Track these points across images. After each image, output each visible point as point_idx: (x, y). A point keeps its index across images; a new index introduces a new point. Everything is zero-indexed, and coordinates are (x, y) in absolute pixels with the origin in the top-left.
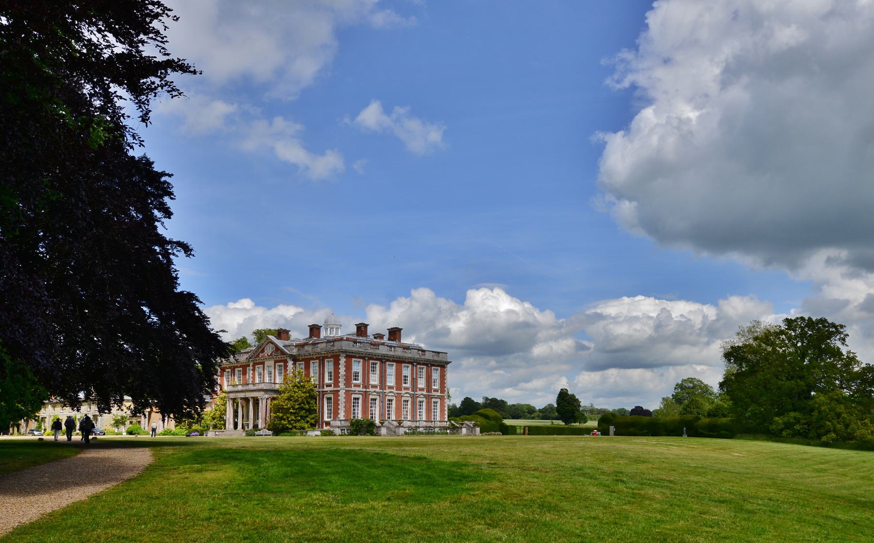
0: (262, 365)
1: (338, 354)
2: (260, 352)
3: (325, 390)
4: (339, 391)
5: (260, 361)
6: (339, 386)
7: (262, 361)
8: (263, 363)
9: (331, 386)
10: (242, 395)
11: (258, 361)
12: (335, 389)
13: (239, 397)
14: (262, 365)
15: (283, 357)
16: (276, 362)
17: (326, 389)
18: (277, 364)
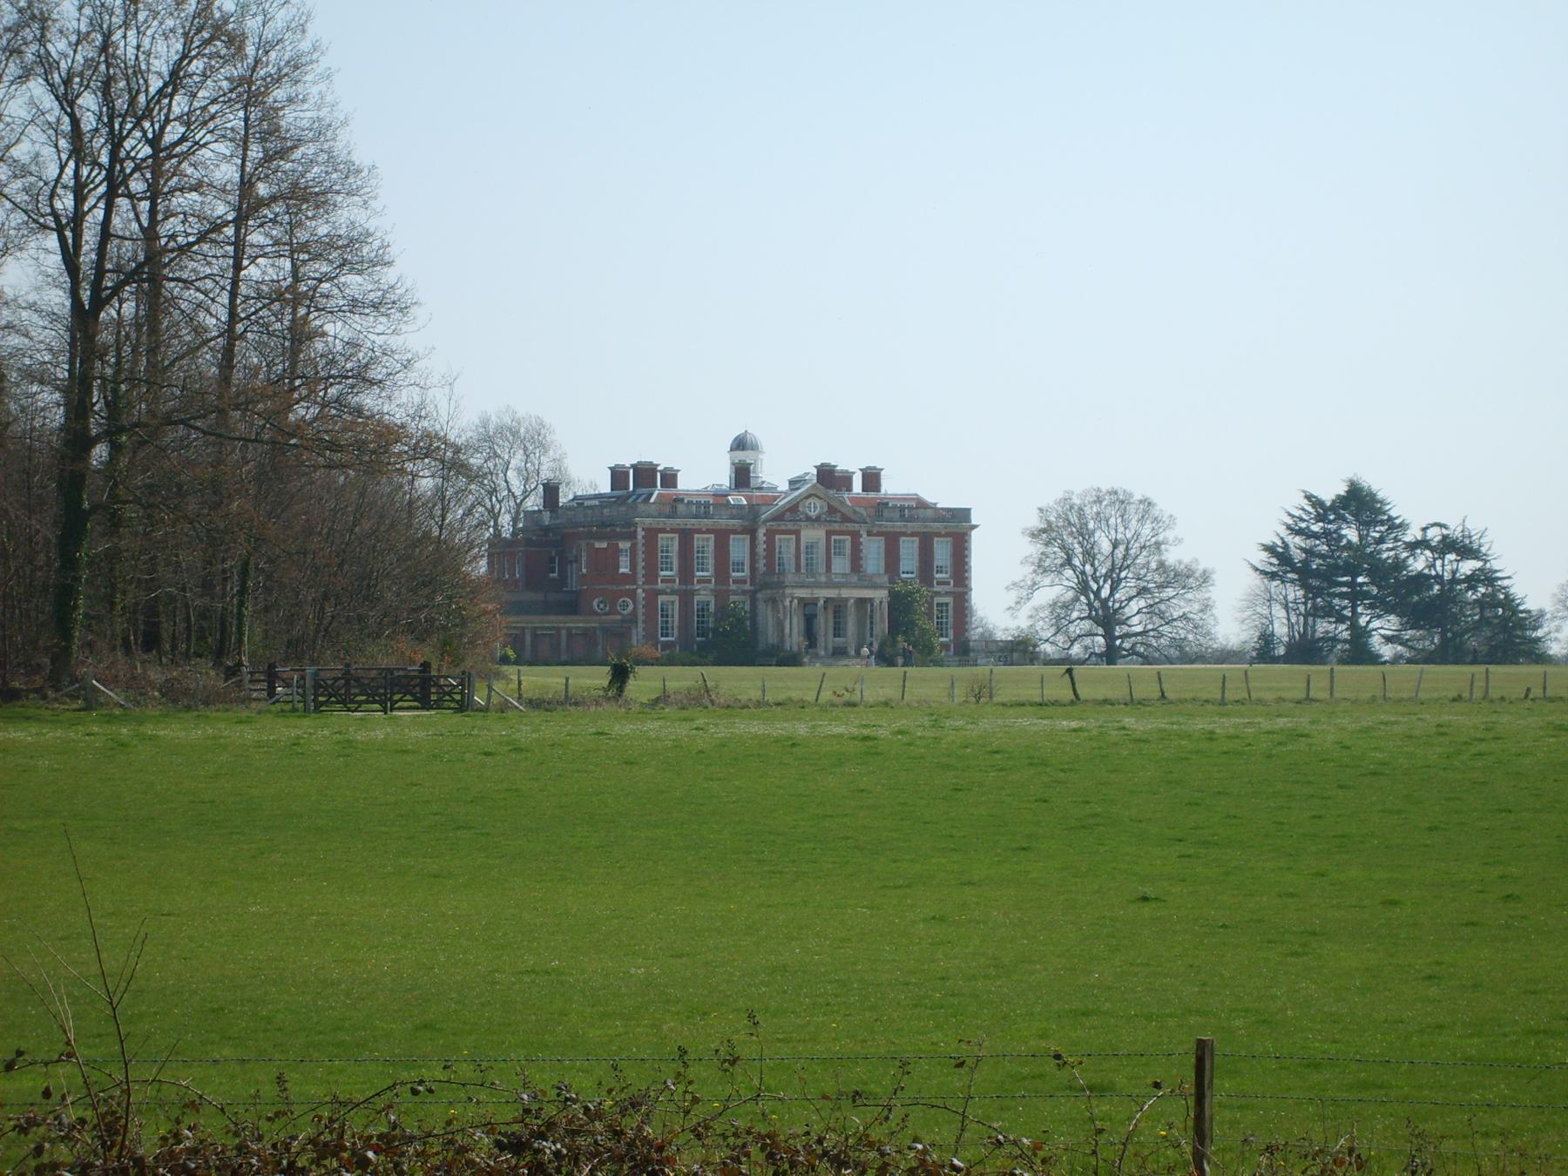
0: (793, 537)
1: (963, 531)
2: (787, 510)
3: (935, 590)
4: (966, 593)
5: (790, 526)
6: (966, 586)
7: (795, 528)
8: (797, 533)
9: (948, 583)
10: (832, 593)
11: (783, 528)
12: (960, 590)
13: (821, 595)
14: (793, 537)
15: (850, 526)
16: (829, 534)
17: (937, 588)
18: (833, 537)
